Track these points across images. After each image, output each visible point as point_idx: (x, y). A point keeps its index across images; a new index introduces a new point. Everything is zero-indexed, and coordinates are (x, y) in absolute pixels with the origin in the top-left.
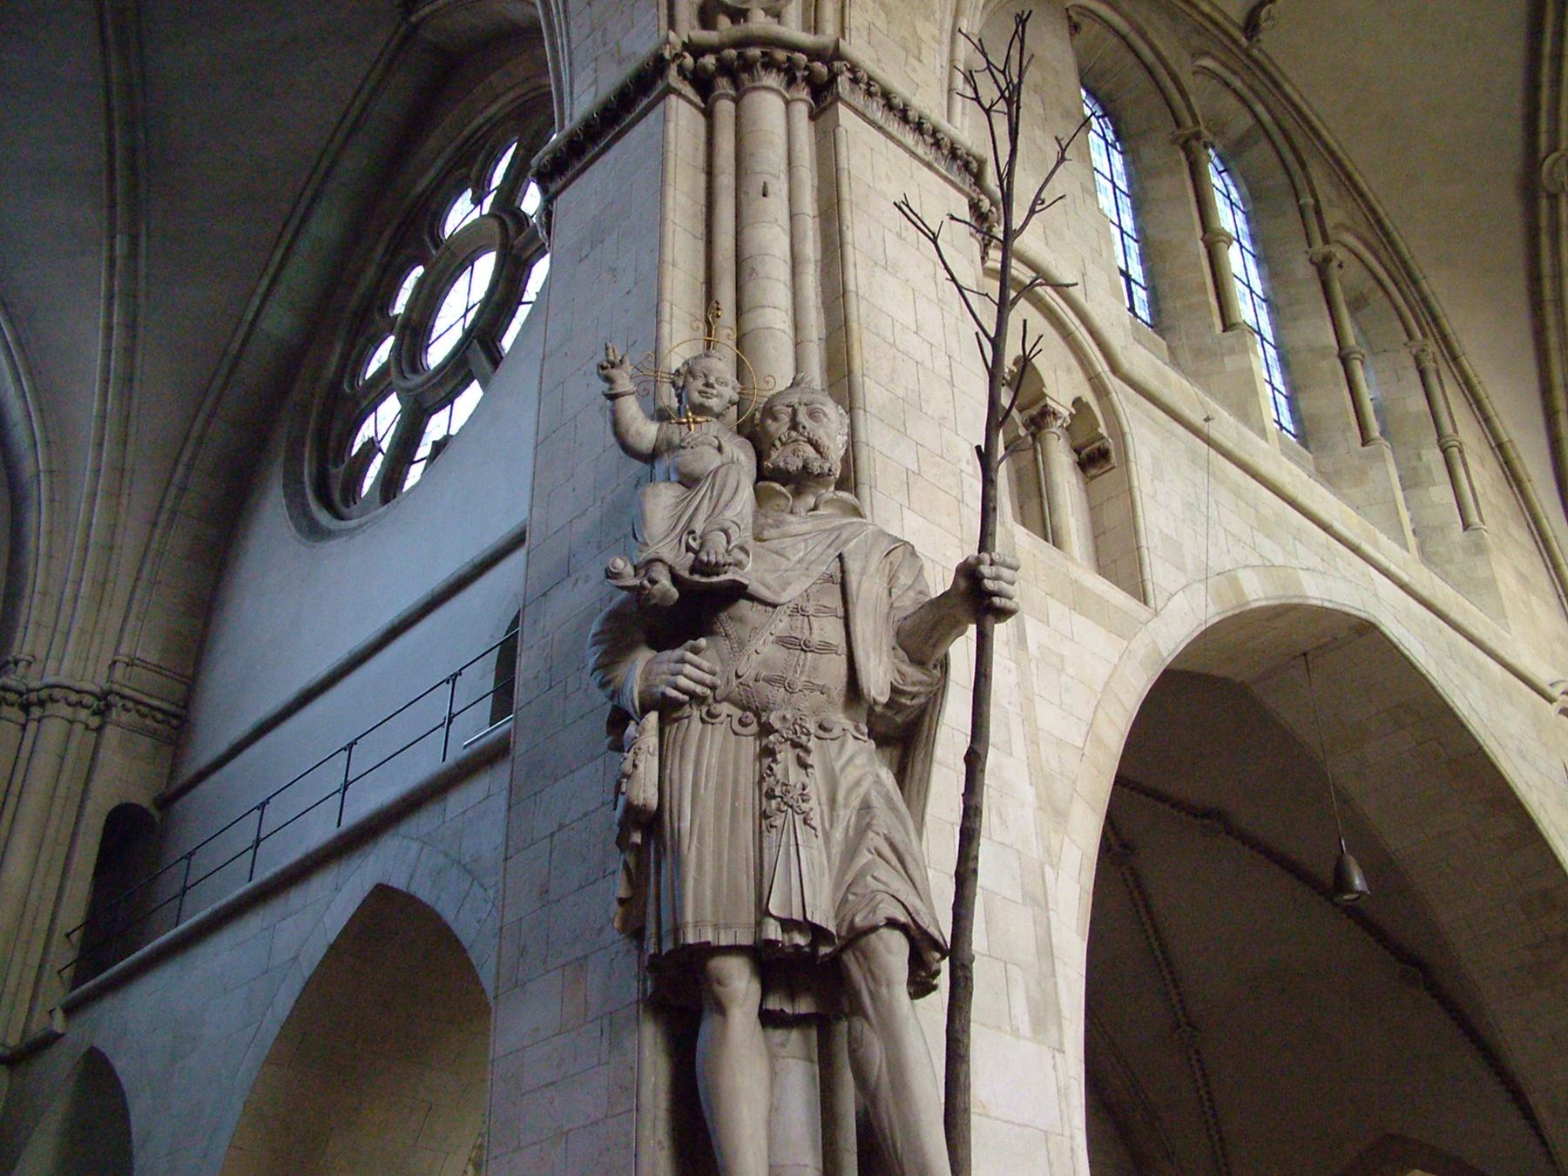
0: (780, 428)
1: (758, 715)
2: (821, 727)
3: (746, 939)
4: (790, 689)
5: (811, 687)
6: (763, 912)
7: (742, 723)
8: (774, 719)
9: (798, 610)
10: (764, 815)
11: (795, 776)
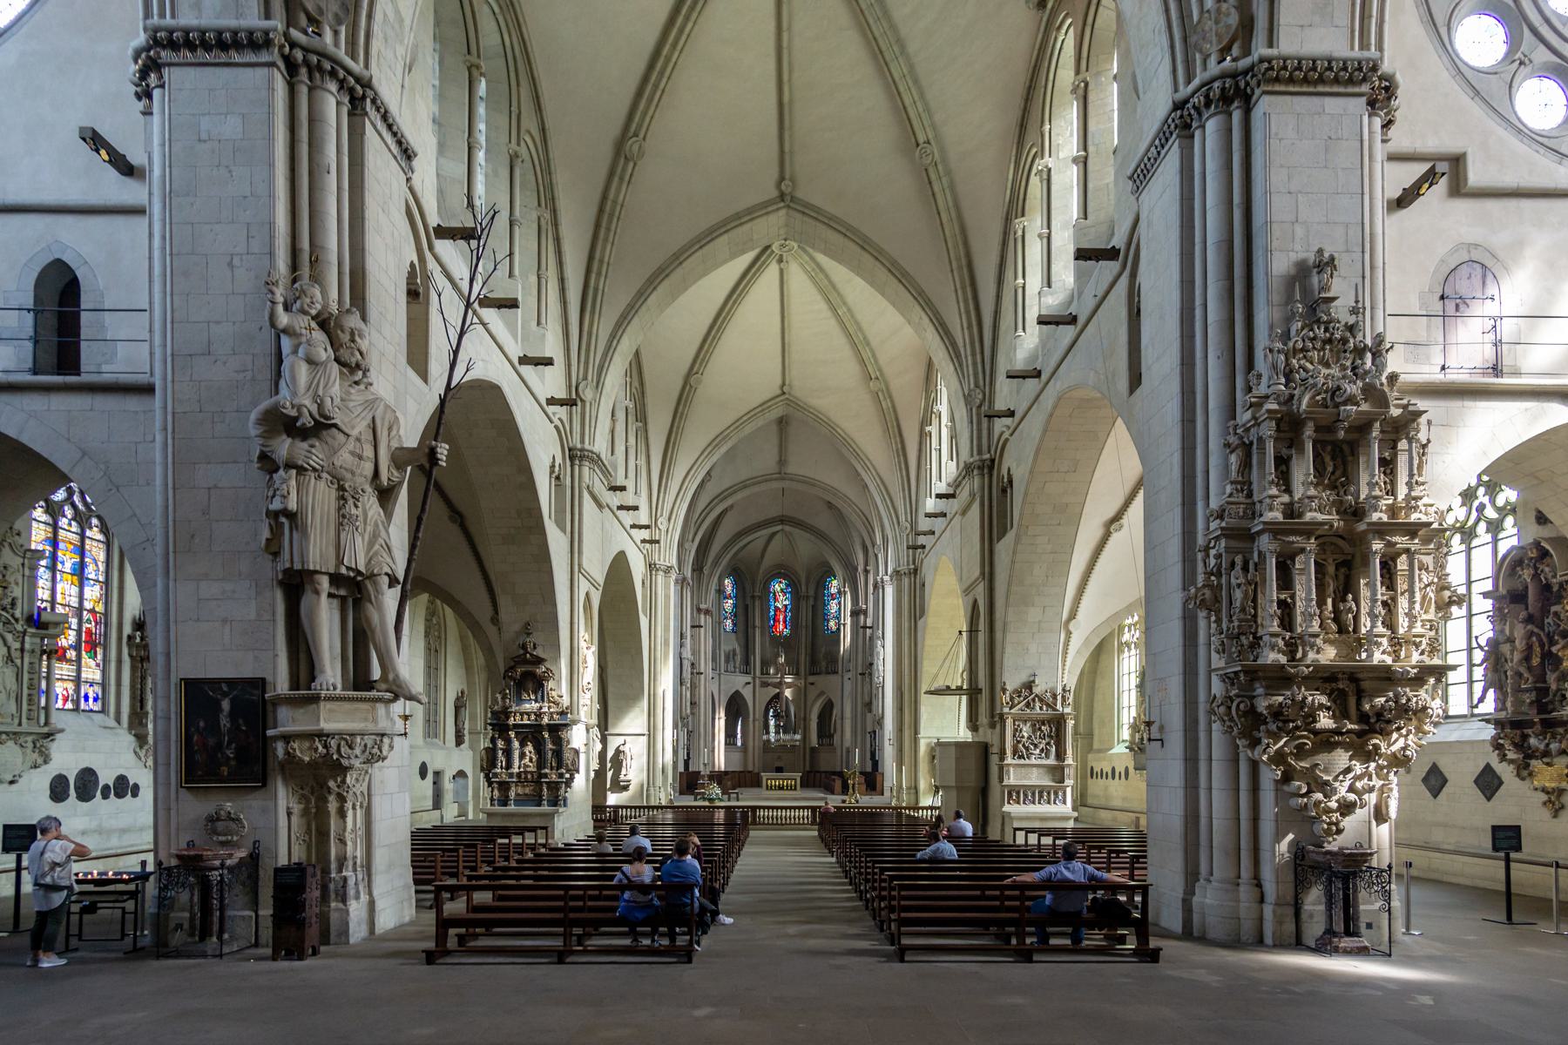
0: (345, 338)
1: (338, 481)
2: (362, 490)
3: (332, 571)
4: (353, 473)
5: (361, 475)
6: (340, 561)
7: (331, 482)
8: (347, 486)
9: (358, 440)
10: (341, 524)
11: (354, 511)
